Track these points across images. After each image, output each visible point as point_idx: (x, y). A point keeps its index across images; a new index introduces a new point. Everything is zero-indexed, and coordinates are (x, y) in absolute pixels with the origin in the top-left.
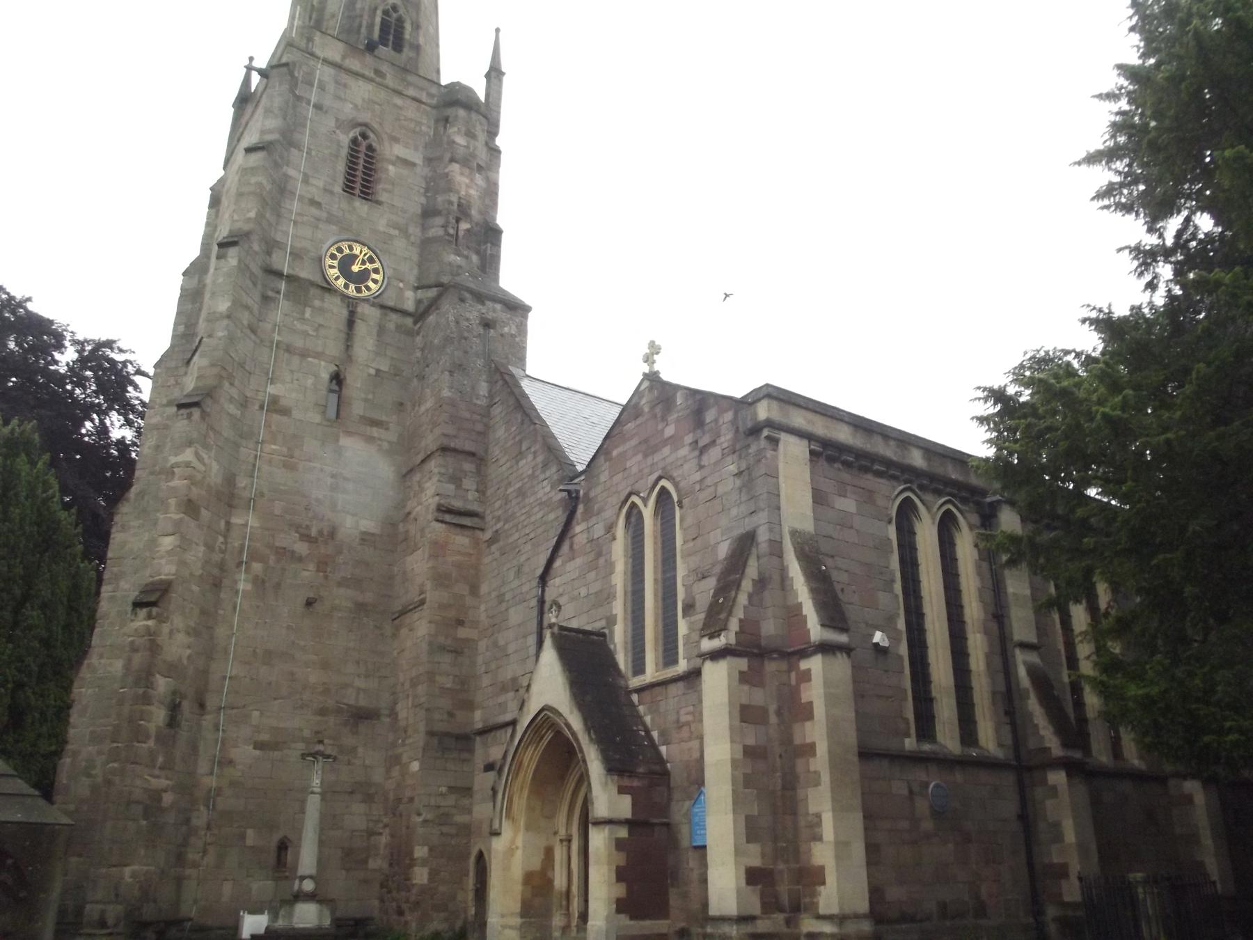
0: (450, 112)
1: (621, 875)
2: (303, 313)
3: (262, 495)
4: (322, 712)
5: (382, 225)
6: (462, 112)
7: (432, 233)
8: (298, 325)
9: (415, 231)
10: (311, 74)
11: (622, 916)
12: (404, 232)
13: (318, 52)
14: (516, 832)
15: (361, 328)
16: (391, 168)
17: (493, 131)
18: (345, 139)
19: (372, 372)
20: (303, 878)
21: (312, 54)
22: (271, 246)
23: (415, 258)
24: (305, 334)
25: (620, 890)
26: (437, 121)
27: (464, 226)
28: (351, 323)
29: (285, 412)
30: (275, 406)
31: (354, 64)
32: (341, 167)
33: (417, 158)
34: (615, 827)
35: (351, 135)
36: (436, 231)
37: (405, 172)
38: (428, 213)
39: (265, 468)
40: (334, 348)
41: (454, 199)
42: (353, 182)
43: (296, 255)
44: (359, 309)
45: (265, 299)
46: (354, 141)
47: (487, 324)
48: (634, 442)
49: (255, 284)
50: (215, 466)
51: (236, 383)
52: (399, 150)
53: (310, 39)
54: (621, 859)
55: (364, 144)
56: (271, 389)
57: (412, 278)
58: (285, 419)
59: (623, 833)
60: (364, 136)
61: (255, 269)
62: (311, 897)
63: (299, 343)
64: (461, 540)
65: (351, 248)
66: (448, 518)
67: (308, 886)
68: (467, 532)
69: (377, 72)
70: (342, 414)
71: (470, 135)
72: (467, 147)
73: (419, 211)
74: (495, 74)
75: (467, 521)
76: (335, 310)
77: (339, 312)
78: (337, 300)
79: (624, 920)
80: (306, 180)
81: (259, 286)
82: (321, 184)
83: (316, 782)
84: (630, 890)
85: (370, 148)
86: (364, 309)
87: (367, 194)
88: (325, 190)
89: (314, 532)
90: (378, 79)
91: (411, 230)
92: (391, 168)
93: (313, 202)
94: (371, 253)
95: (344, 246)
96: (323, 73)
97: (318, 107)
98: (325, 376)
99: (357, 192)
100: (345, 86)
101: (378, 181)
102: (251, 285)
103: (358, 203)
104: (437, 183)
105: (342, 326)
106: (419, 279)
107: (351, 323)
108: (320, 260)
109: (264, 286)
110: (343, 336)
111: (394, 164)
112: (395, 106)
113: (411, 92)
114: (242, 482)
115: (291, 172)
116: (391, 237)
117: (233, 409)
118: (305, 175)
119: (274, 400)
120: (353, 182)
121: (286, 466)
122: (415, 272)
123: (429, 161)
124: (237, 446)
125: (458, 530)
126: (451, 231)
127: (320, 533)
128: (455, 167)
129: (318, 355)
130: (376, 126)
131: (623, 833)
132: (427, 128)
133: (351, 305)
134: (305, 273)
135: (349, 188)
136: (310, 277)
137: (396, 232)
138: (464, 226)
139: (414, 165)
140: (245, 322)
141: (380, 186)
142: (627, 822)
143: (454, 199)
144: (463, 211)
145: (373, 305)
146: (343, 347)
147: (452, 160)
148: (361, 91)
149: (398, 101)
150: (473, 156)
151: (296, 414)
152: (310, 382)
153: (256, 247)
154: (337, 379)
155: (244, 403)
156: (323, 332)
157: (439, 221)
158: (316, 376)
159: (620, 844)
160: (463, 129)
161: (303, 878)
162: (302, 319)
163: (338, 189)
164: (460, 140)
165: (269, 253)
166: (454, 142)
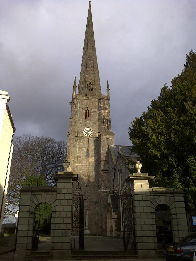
0: (100, 101)
1: (116, 226)
2: (81, 142)
3: (78, 171)
4: (90, 202)
5: (92, 124)
6: (102, 100)
7: (100, 123)
8: (81, 144)
9: (97, 123)
10: (78, 102)
11: (116, 231)
12: (95, 124)
13: (78, 98)
14: (109, 220)
15: (90, 142)
16: (92, 113)
17: (108, 100)
18: (84, 111)
19: (93, 148)
20: (86, 227)
21: (77, 99)
22: (75, 132)
23: (98, 127)
24: (82, 145)
25: (116, 228)
26: (99, 103)
27: (104, 120)
28: (88, 141)
29: (80, 157)
30: (78, 157)
31: (85, 98)
32: (84, 116)
33: (96, 110)
34: (115, 219)
35: (85, 110)
36: (100, 123)
37: (94, 113)
38: (99, 119)
39: (78, 167)
40: (86, 146)
41: (102, 116)
42: (86, 118)
43: (79, 133)
44: (89, 139)
45: (75, 141)
46: (86, 111)
47: (107, 139)
48: (118, 162)
49: (73, 139)
50: (71, 168)
51: (73, 155)
52: (93, 110)
53: (77, 96)
54: (116, 223)
55: (88, 111)
56: (79, 154)
57: (98, 131)
58: (80, 159)
59: (116, 220)
60: (87, 109)
61: (73, 137)
62: (88, 229)
63: (81, 147)
64: (106, 174)
65: (87, 129)
66: (103, 171)
67: (87, 228)
68: (107, 173)
69: (88, 98)
70: (89, 156)
71: (104, 104)
72: (104, 106)
73: (97, 119)
74: (108, 89)
75: (107, 171)
76: (86, 140)
77: (86, 140)
78: (86, 138)
79: (116, 232)
80: (79, 120)
81: (74, 139)
82: (81, 120)
83: (87, 213)
84: (117, 228)
85: (89, 111)
86: (90, 138)
87: (89, 119)
88: (82, 121)
89: (86, 175)
90: (88, 99)
91: (96, 123)
92: (92, 113)
93: (81, 123)
94: (90, 129)
95: (86, 129)
96: (79, 101)
97: (79, 107)
98: (86, 151)
99: (87, 119)
100: (83, 102)
101: (90, 116)
102: (73, 140)
103: (87, 121)
104: (100, 114)
105: (87, 142)
106: (99, 131)
107: (88, 141)
108: (83, 132)
109: (75, 139)
110: (87, 144)
111: (92, 113)
112: (92, 102)
113: (94, 99)
114: (75, 169)
115: (77, 119)
116: (93, 125)
117: (73, 159)
118: (79, 119)
119: (79, 156)
120: (86, 118)
121: (81, 166)
122: (98, 130)
123: (98, 110)
124: (74, 164)
125: (105, 173)
126: (102, 122)
127: (87, 175)
128: (102, 111)
129: (84, 148)
130: (89, 107)
131: (116, 220)
132: (97, 104)
133: (88, 138)
134: (81, 135)
135: (86, 119)
136: (82, 135)
137: (94, 124)
138: (104, 120)
139: (96, 112)
140: (73, 146)
141: (91, 117)
142: (116, 218)
143: (102, 116)
144: (104, 118)
145: (92, 137)
146: (87, 145)
147: (101, 109)
148: (86, 102)
149: (92, 101)
150: (105, 107)
151: (82, 157)
152: (83, 152)
153: (73, 134)
154: (88, 151)
155: (74, 158)
156: (84, 144)
157: (100, 120)
158: (84, 151)
159: (115, 222)
160: (103, 103)
161: (86, 227)
162: (81, 143)
163: (84, 120)
164: (102, 105)
165: (75, 134)
166: (101, 106)
